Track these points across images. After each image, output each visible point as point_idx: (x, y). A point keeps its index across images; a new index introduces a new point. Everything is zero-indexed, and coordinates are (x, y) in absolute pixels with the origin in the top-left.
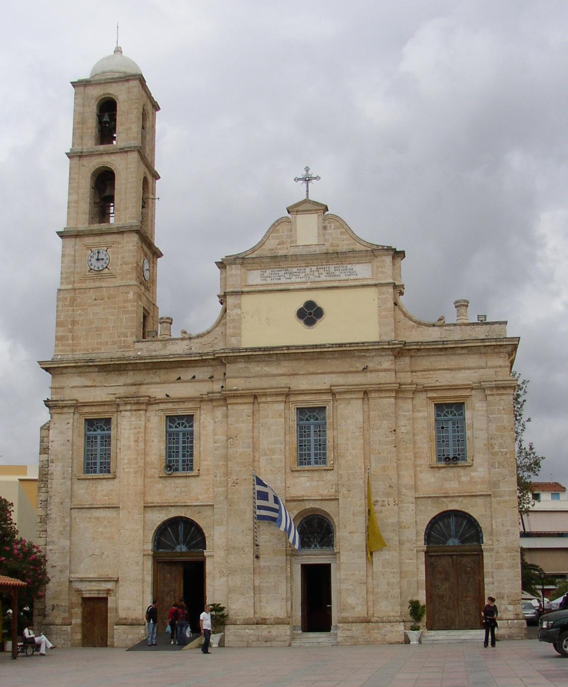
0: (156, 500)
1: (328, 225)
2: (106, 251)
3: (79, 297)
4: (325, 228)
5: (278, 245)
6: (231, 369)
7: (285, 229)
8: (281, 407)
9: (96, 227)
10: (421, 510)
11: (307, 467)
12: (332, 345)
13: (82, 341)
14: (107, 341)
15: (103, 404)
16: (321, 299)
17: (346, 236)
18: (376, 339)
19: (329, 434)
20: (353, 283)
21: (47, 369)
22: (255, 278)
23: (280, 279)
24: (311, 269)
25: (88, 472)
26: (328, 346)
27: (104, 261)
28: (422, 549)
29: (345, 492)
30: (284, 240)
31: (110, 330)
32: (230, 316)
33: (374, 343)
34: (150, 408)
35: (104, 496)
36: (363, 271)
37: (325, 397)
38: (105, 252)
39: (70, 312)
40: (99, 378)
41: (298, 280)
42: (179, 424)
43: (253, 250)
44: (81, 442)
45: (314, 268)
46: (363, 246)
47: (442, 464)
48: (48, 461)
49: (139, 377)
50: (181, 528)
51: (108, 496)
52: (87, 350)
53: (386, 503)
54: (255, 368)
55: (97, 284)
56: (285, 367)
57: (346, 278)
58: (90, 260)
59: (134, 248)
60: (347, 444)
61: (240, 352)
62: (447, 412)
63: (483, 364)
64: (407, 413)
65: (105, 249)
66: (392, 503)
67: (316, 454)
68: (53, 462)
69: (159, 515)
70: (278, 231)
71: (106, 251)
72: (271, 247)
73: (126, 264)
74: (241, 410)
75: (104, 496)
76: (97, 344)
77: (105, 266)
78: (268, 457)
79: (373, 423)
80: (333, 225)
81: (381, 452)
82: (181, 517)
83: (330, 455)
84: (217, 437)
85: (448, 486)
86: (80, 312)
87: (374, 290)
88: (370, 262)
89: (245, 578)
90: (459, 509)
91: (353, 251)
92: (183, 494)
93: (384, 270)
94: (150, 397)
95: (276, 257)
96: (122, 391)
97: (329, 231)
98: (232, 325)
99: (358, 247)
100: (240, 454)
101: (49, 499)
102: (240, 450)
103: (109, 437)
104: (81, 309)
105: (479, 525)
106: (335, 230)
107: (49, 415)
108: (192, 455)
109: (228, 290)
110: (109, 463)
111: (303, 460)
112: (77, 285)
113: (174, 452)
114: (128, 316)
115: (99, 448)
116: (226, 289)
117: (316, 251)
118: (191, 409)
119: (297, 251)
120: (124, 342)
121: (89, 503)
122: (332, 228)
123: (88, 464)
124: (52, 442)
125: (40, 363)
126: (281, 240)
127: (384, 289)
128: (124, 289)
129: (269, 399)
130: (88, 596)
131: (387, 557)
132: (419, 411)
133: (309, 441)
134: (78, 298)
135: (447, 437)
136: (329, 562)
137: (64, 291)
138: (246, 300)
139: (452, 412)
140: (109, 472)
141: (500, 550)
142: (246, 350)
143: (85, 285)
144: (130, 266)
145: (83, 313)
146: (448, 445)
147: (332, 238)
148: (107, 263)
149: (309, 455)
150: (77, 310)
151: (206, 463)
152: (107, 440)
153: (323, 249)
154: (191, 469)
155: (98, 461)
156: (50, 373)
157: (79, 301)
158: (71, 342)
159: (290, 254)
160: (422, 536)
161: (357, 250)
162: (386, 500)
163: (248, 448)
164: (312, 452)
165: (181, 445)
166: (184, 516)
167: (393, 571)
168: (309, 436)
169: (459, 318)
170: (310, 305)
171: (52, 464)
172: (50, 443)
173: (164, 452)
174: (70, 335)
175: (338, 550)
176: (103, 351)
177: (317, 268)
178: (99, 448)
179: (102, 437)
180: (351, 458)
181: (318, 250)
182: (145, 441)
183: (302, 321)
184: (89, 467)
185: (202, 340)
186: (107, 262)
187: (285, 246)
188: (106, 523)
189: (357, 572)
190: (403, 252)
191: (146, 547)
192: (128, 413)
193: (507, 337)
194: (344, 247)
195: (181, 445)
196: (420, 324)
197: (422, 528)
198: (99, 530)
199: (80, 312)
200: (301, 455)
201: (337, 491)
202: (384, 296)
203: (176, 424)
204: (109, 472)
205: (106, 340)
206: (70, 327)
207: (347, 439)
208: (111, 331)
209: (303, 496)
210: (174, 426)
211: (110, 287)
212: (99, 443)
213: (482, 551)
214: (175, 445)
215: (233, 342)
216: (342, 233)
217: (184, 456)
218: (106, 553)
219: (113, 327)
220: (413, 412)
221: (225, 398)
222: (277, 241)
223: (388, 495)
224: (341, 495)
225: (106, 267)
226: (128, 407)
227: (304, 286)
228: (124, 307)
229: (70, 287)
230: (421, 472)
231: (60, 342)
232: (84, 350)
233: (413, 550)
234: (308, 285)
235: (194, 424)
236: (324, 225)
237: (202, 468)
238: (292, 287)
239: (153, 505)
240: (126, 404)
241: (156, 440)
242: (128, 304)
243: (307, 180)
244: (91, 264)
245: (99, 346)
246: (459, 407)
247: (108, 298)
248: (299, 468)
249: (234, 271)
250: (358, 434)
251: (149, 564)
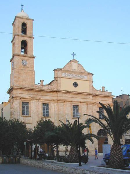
6: (59, 94)
8: (70, 104)
15: (28, 98)
16: (78, 82)
20: (83, 79)
22: (63, 75)
25: (23, 115)
34: (39, 101)
36: (86, 77)
37: (79, 103)
40: (26, 92)
43: (63, 68)
45: (76, 75)
49: (36, 93)
54: (65, 95)
63: (108, 100)
74: (61, 104)
87: (88, 81)
91: (84, 73)
95: (69, 71)
96: (32, 96)
99: (85, 72)
119: (73, 70)
123: (23, 113)
127: (91, 82)
129: (67, 102)
152: (28, 108)
153: (78, 71)
155: (25, 112)
170: (75, 83)
179: (26, 107)
181: (77, 71)
182: (38, 109)
184: (23, 114)
192: (34, 102)
193: (112, 95)
194: (82, 71)
196: (96, 90)
212: (25, 108)
215: (59, 88)
221: (58, 101)
222: (68, 67)
226: (34, 100)
234: (75, 78)
237: (51, 116)
238: (72, 78)
240: (34, 99)
241: (40, 109)
243: (74, 55)
249: (59, 72)
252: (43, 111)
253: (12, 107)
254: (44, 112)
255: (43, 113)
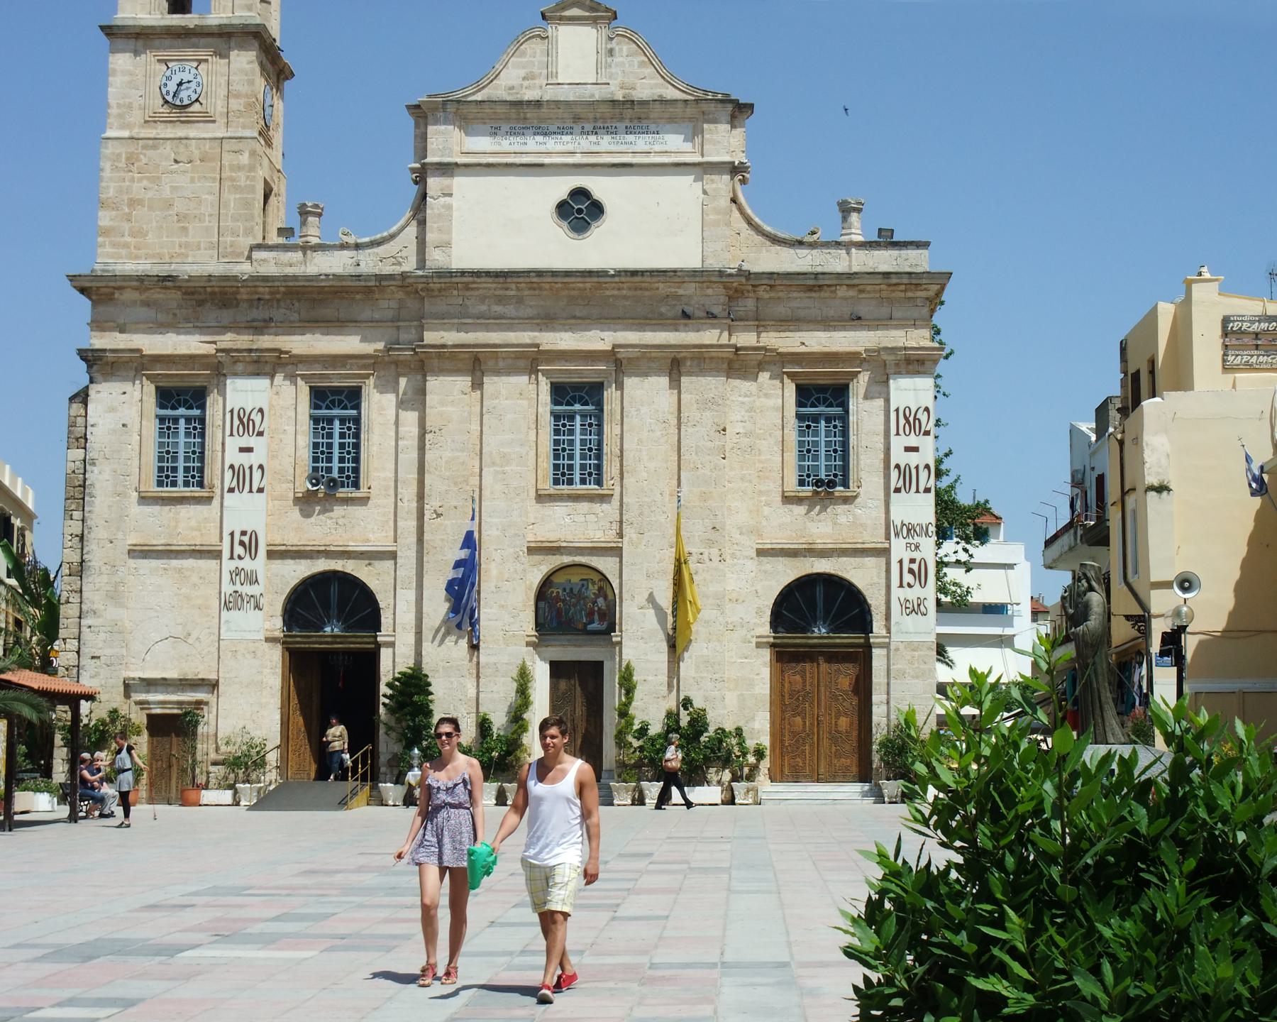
0: (292, 539)
1: (617, 48)
2: (196, 68)
3: (145, 155)
4: (611, 52)
5: (524, 79)
7: (538, 51)
9: (177, 20)
10: (765, 572)
11: (565, 489)
12: (619, 273)
13: (151, 238)
14: (200, 242)
16: (599, 186)
17: (649, 70)
18: (694, 263)
19: (611, 431)
21: (83, 291)
23: (526, 144)
24: (583, 128)
26: (612, 272)
27: (193, 85)
28: (765, 640)
29: (634, 536)
30: (535, 70)
31: (205, 221)
32: (432, 209)
33: (694, 273)
35: (193, 529)
38: (194, 71)
39: (127, 183)
41: (560, 148)
42: (333, 402)
44: (152, 427)
46: (677, 91)
47: (808, 490)
48: (85, 461)
50: (334, 590)
51: (200, 530)
52: (160, 256)
53: (705, 557)
55: (181, 131)
56: (531, 307)
57: (647, 148)
58: (166, 85)
59: (250, 66)
60: (641, 451)
61: (451, 277)
62: (818, 399)
64: (747, 399)
65: (195, 64)
66: (716, 559)
67: (583, 467)
68: (94, 464)
69: (294, 567)
70: (523, 54)
71: (196, 68)
72: (511, 83)
73: (238, 96)
75: (193, 529)
76: (180, 246)
77: (194, 97)
78: (498, 469)
79: (687, 414)
80: (625, 48)
81: (700, 466)
82: (335, 573)
83: (610, 468)
84: (406, 429)
85: (815, 531)
86: (145, 183)
88: (691, 119)
89: (452, 683)
90: (833, 572)
92: (340, 530)
93: (715, 137)
94: (281, 352)
97: (618, 59)
98: (435, 226)
100: (446, 462)
101: (86, 532)
102: (447, 454)
103: (202, 420)
104: (148, 178)
105: (865, 601)
106: (630, 58)
107: (88, 377)
108: (356, 460)
109: (430, 159)
110: (201, 470)
111: (562, 475)
112: (135, 132)
113: (323, 453)
114: (238, 196)
115: (182, 439)
116: (425, 157)
117: (593, 95)
118: (360, 376)
120: (231, 246)
121: (163, 542)
122: (625, 53)
123: (161, 469)
124: (92, 426)
125: (72, 278)
126: (527, 70)
128: (234, 145)
130: (159, 711)
131: (705, 652)
132: (766, 395)
133: (571, 442)
134: (142, 157)
135: (816, 444)
136: (600, 659)
137: (115, 142)
138: (460, 183)
139: (825, 400)
140: (201, 484)
141: (901, 647)
142: (463, 273)
143: (154, 131)
144: (242, 101)
145: (151, 185)
146: (816, 458)
147: (623, 71)
148: (198, 91)
149: (571, 467)
150: (140, 180)
151: (382, 475)
152: (199, 426)
154: (356, 485)
155: (181, 464)
156: (90, 298)
157: (144, 162)
158: (128, 239)
159: (546, 98)
160: (767, 617)
161: (669, 98)
162: (706, 552)
163: (463, 451)
164: (577, 462)
165: (336, 440)
166: (340, 569)
167: (717, 676)
168: (571, 432)
169: (844, 231)
170: (580, 194)
171: (96, 469)
172: (89, 429)
173: (305, 454)
174: (126, 226)
175: (619, 639)
176: (190, 260)
177: (594, 128)
178: (182, 439)
180: (645, 474)
183: (565, 224)
184: (165, 476)
185: (380, 250)
186: (199, 90)
187: (537, 82)
188: (195, 579)
189: (650, 678)
190: (751, 106)
191: (268, 625)
195: (336, 440)
197: (766, 603)
198: (183, 591)
199: (145, 183)
200: (556, 467)
201: (621, 535)
202: (714, 186)
203: (328, 402)
204: (201, 484)
205: (198, 240)
206: (127, 210)
207: (640, 441)
208: (207, 223)
209: (559, 540)
210: (324, 406)
211: (204, 139)
213: (868, 648)
214: (325, 440)
215: (436, 258)
216: (641, 64)
217: (342, 460)
218: (194, 635)
219: (211, 215)
220: (759, 397)
222: (522, 73)
223: (710, 543)
224: (626, 539)
225: (197, 100)
227: (570, 160)
228: (232, 179)
229: (126, 134)
230: (768, 504)
231: (107, 239)
232: (153, 256)
233: (750, 642)
235: (363, 404)
236: (609, 46)
238: (547, 160)
239: (283, 548)
242: (239, 174)
244: (168, 93)
245: (183, 251)
246: (837, 394)
247: (202, 161)
248: (552, 491)
250: (659, 433)
251: (275, 656)
252: (316, 445)
253: (79, 431)
254: (320, 452)
255: (316, 460)
